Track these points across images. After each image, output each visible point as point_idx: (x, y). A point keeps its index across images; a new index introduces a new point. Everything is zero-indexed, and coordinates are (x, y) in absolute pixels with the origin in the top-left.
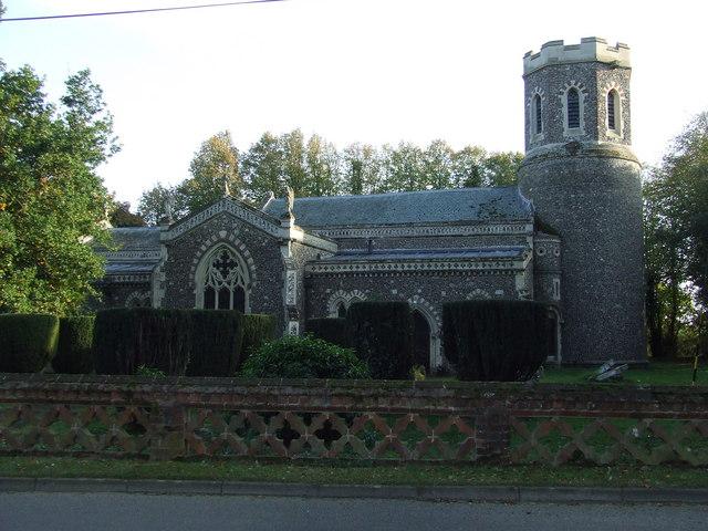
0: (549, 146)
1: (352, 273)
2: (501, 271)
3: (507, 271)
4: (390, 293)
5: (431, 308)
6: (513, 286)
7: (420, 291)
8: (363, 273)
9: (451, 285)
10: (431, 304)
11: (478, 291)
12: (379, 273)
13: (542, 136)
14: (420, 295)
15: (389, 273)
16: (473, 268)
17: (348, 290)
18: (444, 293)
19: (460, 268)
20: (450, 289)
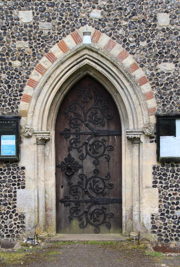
4: (14, 22)
5: (129, 61)
7: (96, 14)
10: (129, 49)
14: (99, 24)
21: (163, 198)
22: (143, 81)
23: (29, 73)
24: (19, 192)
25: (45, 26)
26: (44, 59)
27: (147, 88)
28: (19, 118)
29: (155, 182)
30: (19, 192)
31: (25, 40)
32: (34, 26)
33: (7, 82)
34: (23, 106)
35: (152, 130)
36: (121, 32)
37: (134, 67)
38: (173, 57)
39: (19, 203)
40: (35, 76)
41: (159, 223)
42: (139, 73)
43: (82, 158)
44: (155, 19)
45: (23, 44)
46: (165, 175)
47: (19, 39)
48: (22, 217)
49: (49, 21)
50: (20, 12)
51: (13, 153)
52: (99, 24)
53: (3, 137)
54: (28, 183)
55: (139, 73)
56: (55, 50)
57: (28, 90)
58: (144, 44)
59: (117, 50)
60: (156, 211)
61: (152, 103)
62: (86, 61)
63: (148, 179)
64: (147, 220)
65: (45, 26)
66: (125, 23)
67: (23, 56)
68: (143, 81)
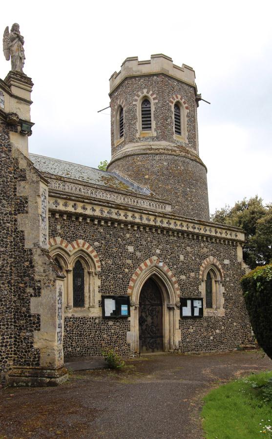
0: (163, 144)
1: (78, 215)
2: (229, 240)
3: (233, 240)
6: (236, 256)
7: (158, 251)
8: (93, 218)
9: (188, 249)
10: (170, 269)
11: (211, 258)
12: (113, 221)
13: (153, 133)
14: (159, 256)
15: (126, 223)
16: (208, 233)
17: (71, 239)
18: (182, 258)
19: (196, 231)
20: (187, 253)
21: (183, 334)
22: (175, 283)
23: (132, 275)
24: (128, 332)
25: (138, 254)
26: (138, 269)
27: (176, 286)
28: (129, 297)
29: (180, 327)
30: (128, 332)
31: (130, 259)
32: (134, 254)
33: (122, 279)
34: (129, 291)
35: (179, 304)
36: (167, 260)
37: (172, 276)
38: (185, 273)
39: (128, 338)
40: (134, 277)
41: (181, 344)
42: (174, 279)
43: (147, 316)
44: (179, 257)
45: (129, 262)
46: (183, 324)
47: (128, 259)
48: (129, 345)
49: (140, 252)
50: (129, 247)
51: (127, 314)
52: (159, 256)
53: (122, 306)
54: (132, 328)
55: (174, 279)
56: (142, 265)
57: (131, 284)
58: (175, 267)
59: (166, 268)
60: (180, 339)
61: (178, 292)
62: (154, 272)
63: (177, 326)
64: (177, 344)
65: (138, 254)
66: (169, 257)
67: (129, 267)
68: (175, 283)
